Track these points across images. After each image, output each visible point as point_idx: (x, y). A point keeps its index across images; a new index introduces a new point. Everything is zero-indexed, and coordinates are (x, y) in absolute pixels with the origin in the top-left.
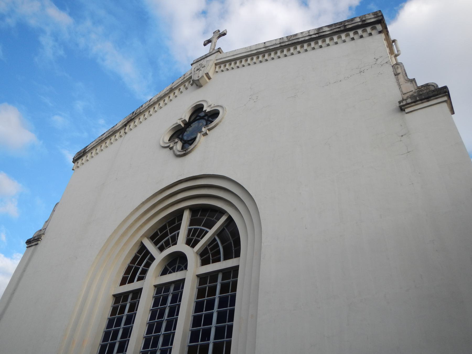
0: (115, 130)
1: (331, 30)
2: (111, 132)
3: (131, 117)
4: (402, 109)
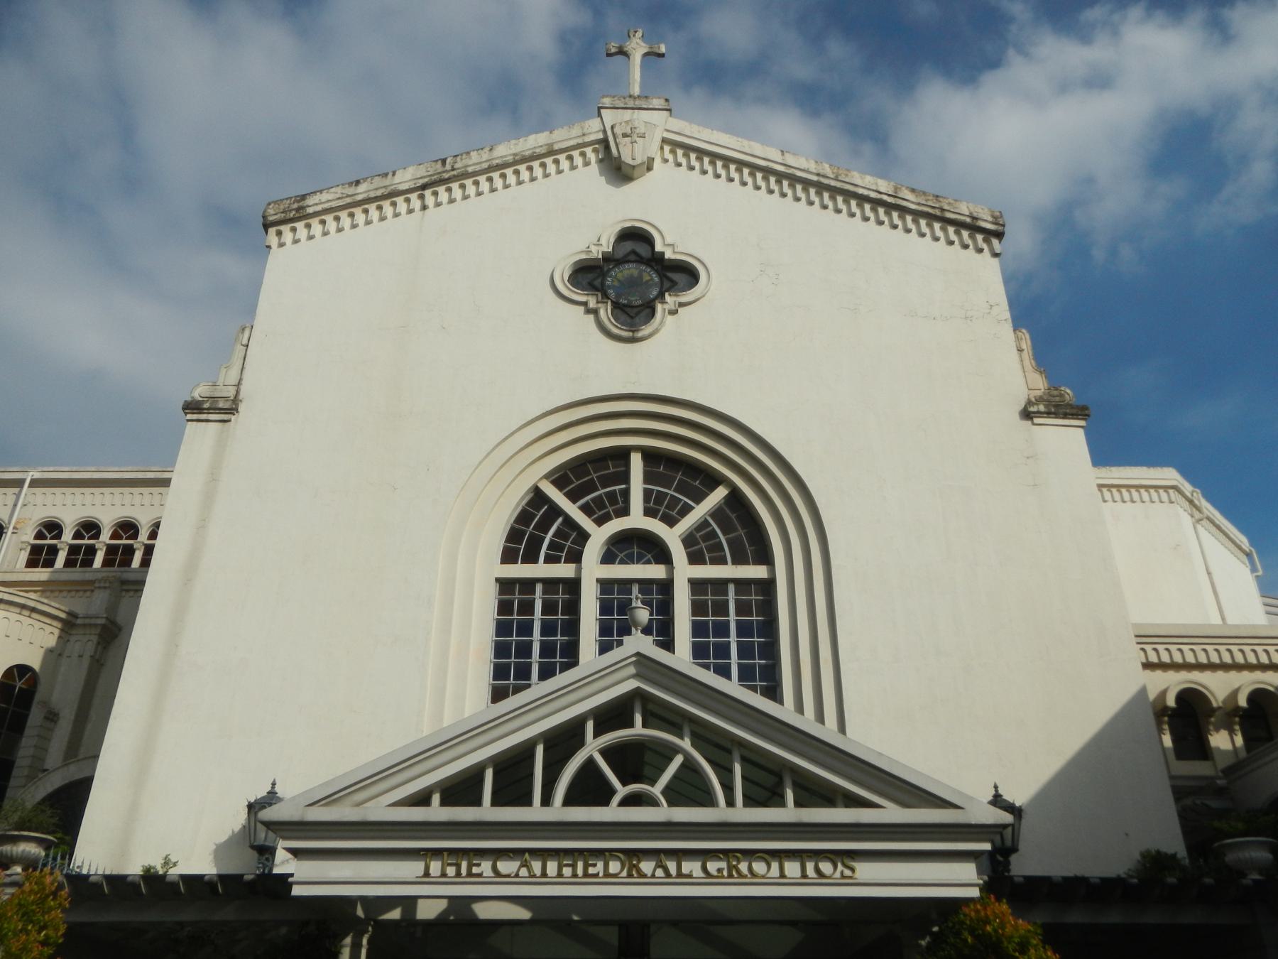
0: (392, 187)
1: (919, 204)
2: (381, 188)
3: (439, 173)
4: (1027, 415)
